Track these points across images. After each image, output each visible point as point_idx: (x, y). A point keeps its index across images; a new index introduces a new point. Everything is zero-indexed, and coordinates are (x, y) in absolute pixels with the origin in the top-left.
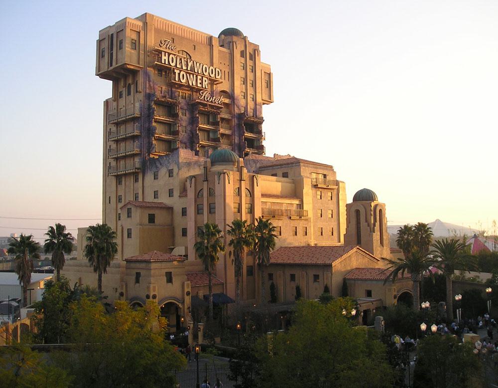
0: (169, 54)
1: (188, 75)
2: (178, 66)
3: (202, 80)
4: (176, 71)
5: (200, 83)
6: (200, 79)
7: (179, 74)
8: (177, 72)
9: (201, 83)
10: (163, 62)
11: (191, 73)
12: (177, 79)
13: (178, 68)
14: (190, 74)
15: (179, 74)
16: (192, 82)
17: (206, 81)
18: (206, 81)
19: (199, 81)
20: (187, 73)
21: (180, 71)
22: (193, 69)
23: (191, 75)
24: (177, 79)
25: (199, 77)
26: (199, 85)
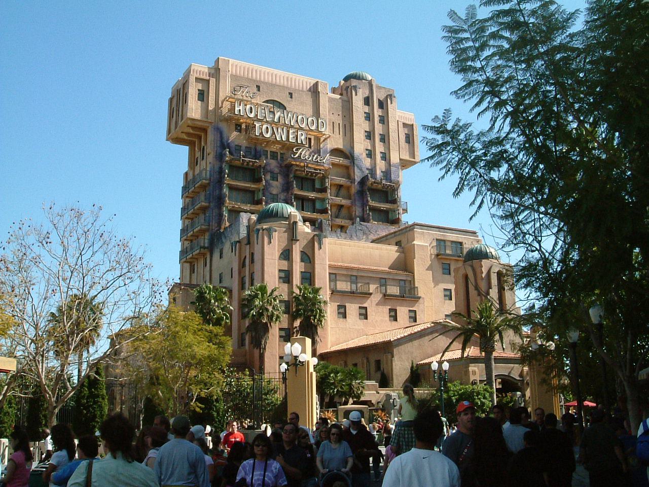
13: (259, 120)
16: (281, 135)
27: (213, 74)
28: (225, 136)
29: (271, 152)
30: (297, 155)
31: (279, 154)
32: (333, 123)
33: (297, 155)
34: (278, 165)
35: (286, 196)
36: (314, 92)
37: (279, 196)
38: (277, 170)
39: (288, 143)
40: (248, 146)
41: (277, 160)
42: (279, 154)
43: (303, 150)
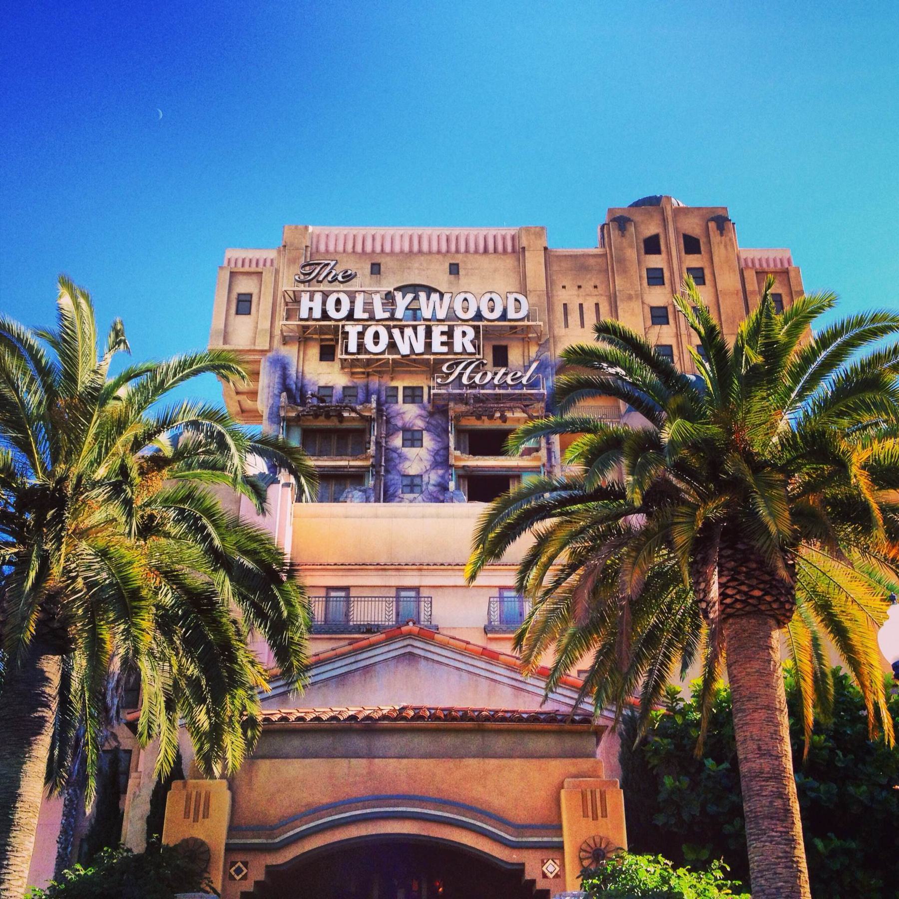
0: (326, 295)
1: (396, 332)
2: (359, 314)
3: (450, 334)
4: (347, 329)
5: (443, 344)
6: (443, 333)
7: (361, 335)
8: (353, 330)
9: (449, 344)
10: (304, 314)
11: (408, 326)
12: (353, 347)
14: (402, 329)
15: (361, 335)
17: (464, 334)
18: (464, 334)
19: (437, 339)
20: (388, 328)
21: (365, 328)
22: (414, 312)
23: (409, 332)
24: (353, 347)
25: (437, 331)
26: (437, 347)
27: (272, 260)
28: (293, 372)
29: (405, 388)
30: (451, 378)
31: (426, 390)
32: (565, 305)
33: (451, 378)
34: (423, 413)
35: (442, 477)
36: (514, 251)
37: (425, 479)
38: (420, 424)
39: (432, 357)
40: (350, 384)
41: (422, 402)
42: (426, 390)
43: (465, 368)
